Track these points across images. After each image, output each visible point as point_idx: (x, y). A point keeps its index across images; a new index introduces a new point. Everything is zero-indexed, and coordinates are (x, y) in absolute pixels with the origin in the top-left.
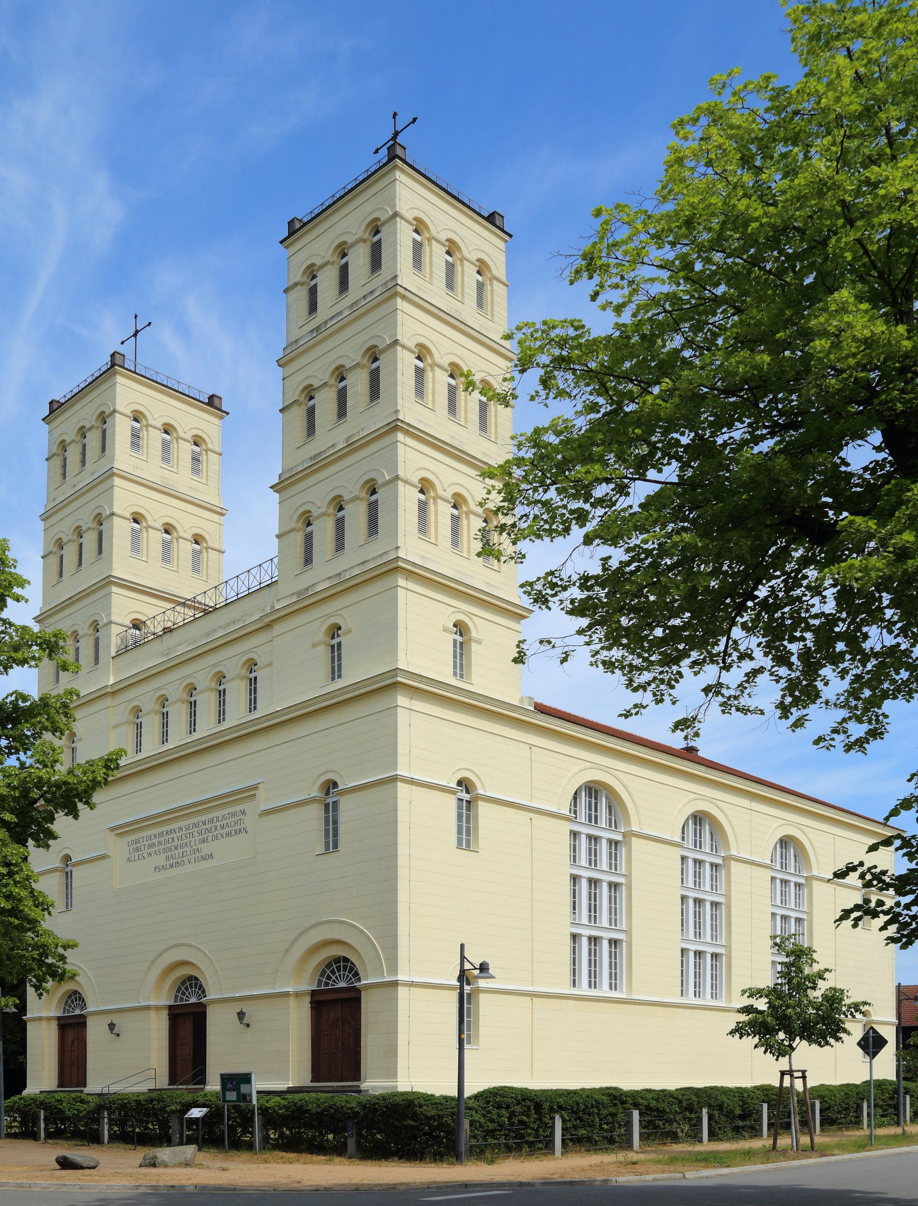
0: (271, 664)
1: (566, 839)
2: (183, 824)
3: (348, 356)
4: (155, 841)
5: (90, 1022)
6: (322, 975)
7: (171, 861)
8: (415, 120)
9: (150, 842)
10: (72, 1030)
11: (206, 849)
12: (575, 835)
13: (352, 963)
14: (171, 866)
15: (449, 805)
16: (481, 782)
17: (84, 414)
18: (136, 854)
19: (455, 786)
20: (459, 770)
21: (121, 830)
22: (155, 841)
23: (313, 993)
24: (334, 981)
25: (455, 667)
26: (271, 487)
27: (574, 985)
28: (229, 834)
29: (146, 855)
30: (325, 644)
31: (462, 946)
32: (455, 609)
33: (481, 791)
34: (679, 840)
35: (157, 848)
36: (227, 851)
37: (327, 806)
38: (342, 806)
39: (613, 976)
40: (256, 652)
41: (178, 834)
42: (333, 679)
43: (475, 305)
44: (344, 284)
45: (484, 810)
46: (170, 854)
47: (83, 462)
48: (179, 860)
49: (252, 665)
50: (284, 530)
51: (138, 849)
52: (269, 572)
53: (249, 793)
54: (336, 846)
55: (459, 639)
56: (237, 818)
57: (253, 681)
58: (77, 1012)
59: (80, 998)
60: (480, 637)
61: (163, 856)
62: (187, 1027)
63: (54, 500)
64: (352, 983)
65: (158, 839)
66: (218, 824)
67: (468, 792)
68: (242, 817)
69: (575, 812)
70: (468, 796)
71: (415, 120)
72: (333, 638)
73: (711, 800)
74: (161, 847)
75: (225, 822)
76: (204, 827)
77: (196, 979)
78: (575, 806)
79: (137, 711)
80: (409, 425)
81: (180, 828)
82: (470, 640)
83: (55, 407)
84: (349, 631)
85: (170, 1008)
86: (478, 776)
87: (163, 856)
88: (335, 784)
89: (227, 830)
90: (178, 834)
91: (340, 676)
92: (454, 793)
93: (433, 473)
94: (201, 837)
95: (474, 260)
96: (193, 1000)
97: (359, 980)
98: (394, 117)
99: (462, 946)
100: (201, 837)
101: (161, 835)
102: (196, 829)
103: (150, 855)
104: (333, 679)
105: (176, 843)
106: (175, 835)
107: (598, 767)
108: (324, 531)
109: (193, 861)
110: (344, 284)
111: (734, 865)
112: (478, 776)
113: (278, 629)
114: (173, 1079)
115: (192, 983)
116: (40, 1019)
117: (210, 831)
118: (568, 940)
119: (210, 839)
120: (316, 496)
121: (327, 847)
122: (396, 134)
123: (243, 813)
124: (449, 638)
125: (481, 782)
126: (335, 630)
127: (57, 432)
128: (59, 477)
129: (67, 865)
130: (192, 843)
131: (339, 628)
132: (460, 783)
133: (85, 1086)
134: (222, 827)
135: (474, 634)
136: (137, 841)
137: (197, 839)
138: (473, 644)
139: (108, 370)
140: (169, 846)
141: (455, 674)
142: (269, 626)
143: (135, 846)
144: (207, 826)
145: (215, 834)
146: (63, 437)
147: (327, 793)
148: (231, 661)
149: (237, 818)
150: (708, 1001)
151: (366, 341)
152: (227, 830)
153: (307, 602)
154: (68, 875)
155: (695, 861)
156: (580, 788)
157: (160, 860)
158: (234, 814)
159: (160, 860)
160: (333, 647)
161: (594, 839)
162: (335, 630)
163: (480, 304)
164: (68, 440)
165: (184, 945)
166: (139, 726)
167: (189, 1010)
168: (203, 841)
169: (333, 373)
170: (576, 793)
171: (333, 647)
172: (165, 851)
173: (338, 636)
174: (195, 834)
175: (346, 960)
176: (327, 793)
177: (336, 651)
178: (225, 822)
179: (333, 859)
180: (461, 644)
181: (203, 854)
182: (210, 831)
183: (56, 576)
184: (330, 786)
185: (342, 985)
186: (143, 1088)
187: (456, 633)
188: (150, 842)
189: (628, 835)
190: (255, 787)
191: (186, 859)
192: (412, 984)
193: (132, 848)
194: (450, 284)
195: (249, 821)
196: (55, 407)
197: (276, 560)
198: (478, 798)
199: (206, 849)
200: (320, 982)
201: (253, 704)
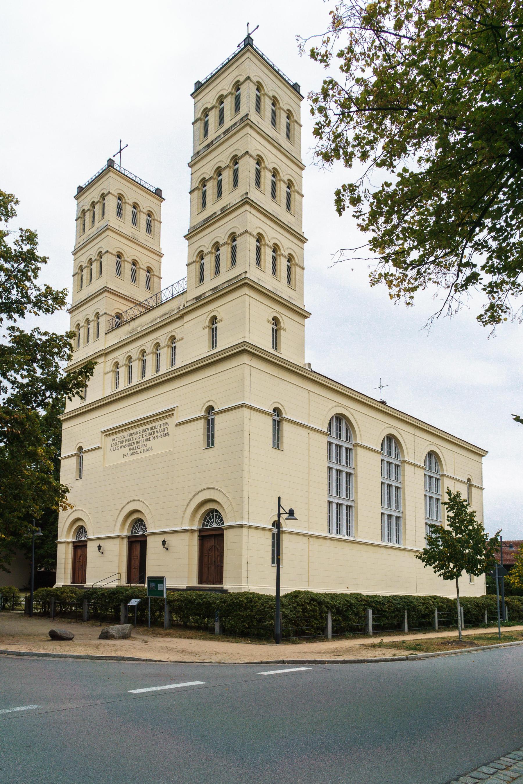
0: (182, 339)
1: (326, 446)
2: (138, 430)
3: (223, 161)
4: (124, 439)
5: (90, 545)
6: (205, 520)
7: (132, 451)
8: (258, 27)
9: (121, 440)
10: (80, 548)
11: (149, 444)
12: (330, 444)
13: (220, 514)
14: (132, 454)
15: (268, 422)
16: (285, 411)
17: (94, 195)
18: (115, 447)
19: (272, 412)
20: (274, 403)
21: (108, 433)
22: (124, 439)
23: (200, 531)
24: (210, 524)
25: (273, 344)
26: (185, 237)
27: (329, 532)
28: (160, 436)
29: (119, 448)
30: (209, 327)
31: (279, 498)
32: (273, 310)
33: (284, 416)
34: (380, 450)
35: (125, 444)
36: (159, 446)
37: (209, 421)
38: (216, 421)
39: (348, 527)
40: (175, 332)
41: (135, 436)
42: (213, 348)
43: (285, 136)
44: (221, 120)
45: (286, 427)
46: (131, 447)
47: (93, 222)
48: (135, 451)
49: (173, 339)
50: (191, 261)
51: (115, 444)
52: (183, 286)
53: (169, 413)
54: (213, 444)
55: (275, 327)
56: (164, 427)
57: (174, 349)
58: (83, 539)
59: (85, 530)
60: (286, 327)
61: (128, 448)
62: (137, 549)
63: (79, 243)
64: (220, 525)
65: (125, 439)
66: (155, 430)
67: (278, 416)
68: (167, 426)
69: (330, 431)
70: (278, 418)
71: (258, 27)
72: (213, 324)
73: (395, 428)
74: (127, 443)
75: (158, 429)
76: (148, 432)
77: (143, 521)
78: (330, 428)
79: (117, 364)
80: (252, 201)
81: (136, 432)
82: (280, 329)
83: (81, 190)
84: (221, 320)
85: (129, 537)
86: (283, 407)
87: (128, 448)
88: (213, 408)
89: (160, 434)
90: (135, 436)
91: (216, 346)
92: (272, 416)
93: (264, 231)
94: (147, 438)
95: (285, 109)
96: (141, 533)
97: (223, 524)
98: (248, 26)
99: (279, 498)
100: (147, 438)
101: (127, 436)
102: (144, 433)
103: (121, 447)
104: (213, 348)
105: (135, 441)
106: (134, 436)
107: (342, 406)
108: (209, 262)
109: (142, 451)
110: (221, 120)
111: (407, 467)
112: (283, 407)
113: (186, 319)
114: (129, 581)
115: (139, 523)
116: (64, 542)
117: (150, 434)
118: (326, 505)
119: (151, 439)
120: (205, 241)
121: (208, 445)
122: (249, 34)
123: (168, 424)
124: (270, 326)
125: (285, 411)
126: (214, 320)
127: (81, 204)
128: (82, 231)
129: (81, 453)
130: (142, 441)
131: (216, 318)
132: (274, 410)
133: (85, 583)
134: (157, 432)
135: (282, 325)
136: (115, 440)
137: (145, 438)
138: (282, 331)
139: (106, 169)
140: (131, 442)
141: (273, 347)
142: (182, 317)
143: (114, 442)
144: (150, 432)
145: (153, 436)
146: (84, 208)
147: (209, 414)
148: (162, 337)
149: (164, 427)
150: (394, 544)
151: (232, 152)
152: (160, 434)
153: (201, 302)
154: (81, 459)
155: (388, 462)
156: (332, 417)
157: (126, 451)
158: (163, 425)
159: (126, 451)
160: (213, 329)
161: (339, 447)
162: (214, 320)
163: (288, 137)
164: (86, 209)
165: (136, 500)
166: (118, 373)
167: (138, 539)
168: (148, 440)
169: (215, 171)
170: (330, 420)
171: (213, 329)
172: (129, 445)
173: (216, 323)
174: (144, 436)
175: (217, 511)
176: (209, 414)
177: (214, 332)
178: (158, 429)
179: (211, 451)
180: (276, 330)
181: (147, 447)
182: (150, 434)
183: (79, 287)
184: (210, 409)
185: (215, 526)
186: (114, 585)
187: (273, 324)
188: (121, 440)
189: (356, 445)
190: (173, 409)
191: (139, 450)
192: (249, 527)
193: (112, 443)
194: (274, 123)
195: (171, 428)
196: (81, 190)
197: (186, 279)
198: (283, 419)
199: (149, 444)
200: (204, 524)
201: (173, 361)
